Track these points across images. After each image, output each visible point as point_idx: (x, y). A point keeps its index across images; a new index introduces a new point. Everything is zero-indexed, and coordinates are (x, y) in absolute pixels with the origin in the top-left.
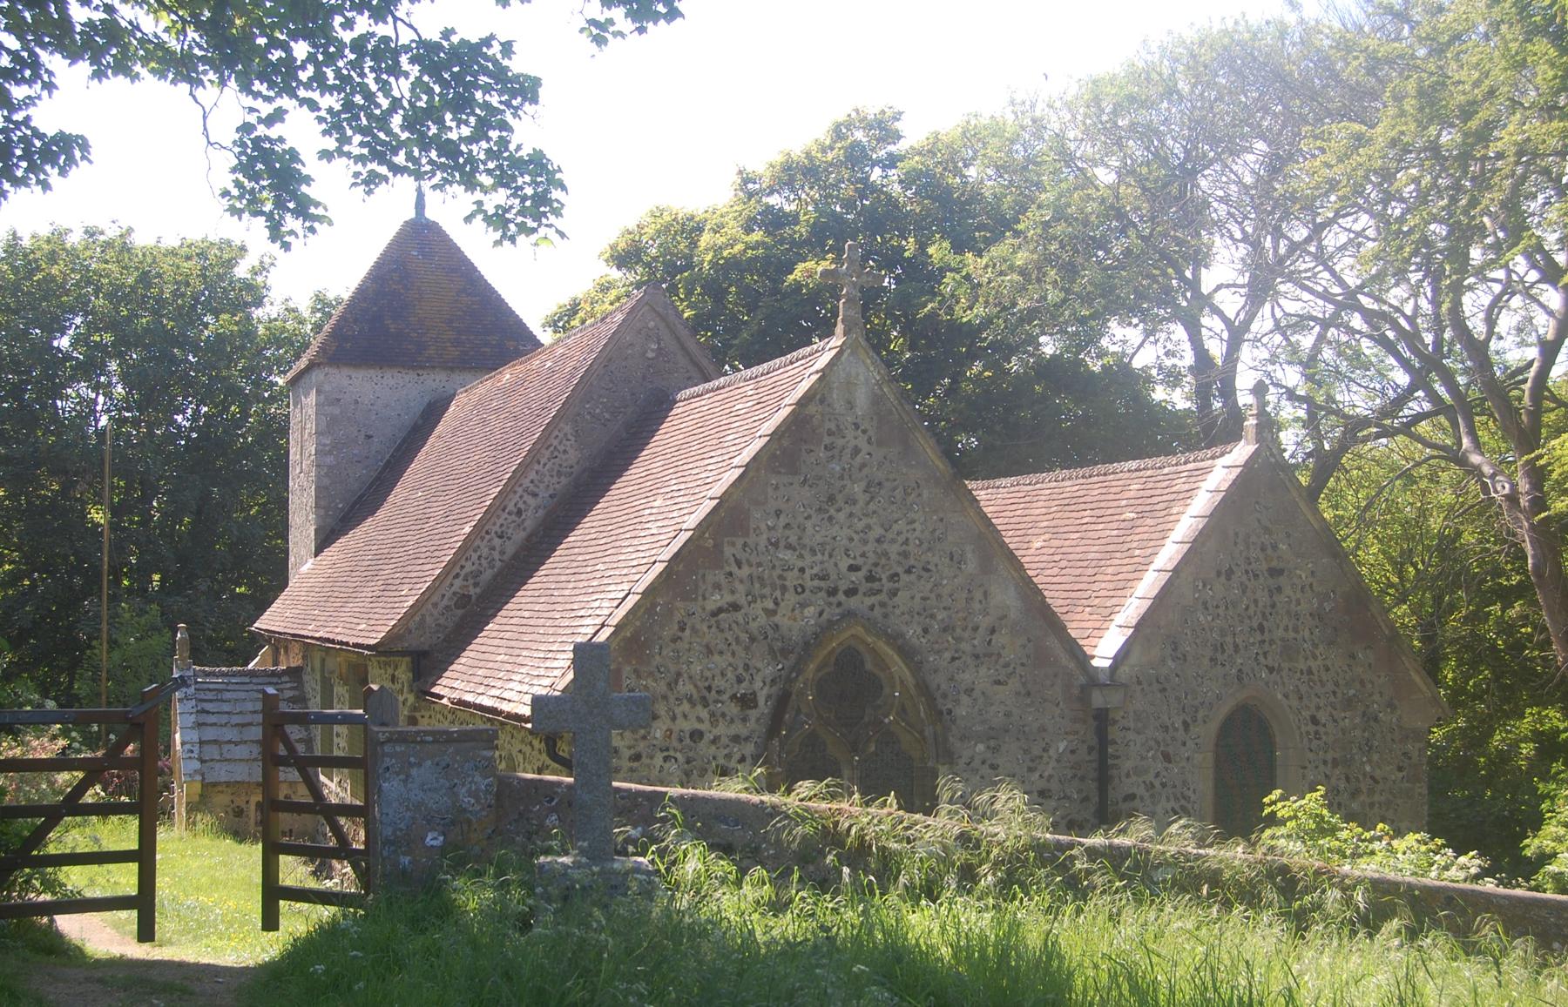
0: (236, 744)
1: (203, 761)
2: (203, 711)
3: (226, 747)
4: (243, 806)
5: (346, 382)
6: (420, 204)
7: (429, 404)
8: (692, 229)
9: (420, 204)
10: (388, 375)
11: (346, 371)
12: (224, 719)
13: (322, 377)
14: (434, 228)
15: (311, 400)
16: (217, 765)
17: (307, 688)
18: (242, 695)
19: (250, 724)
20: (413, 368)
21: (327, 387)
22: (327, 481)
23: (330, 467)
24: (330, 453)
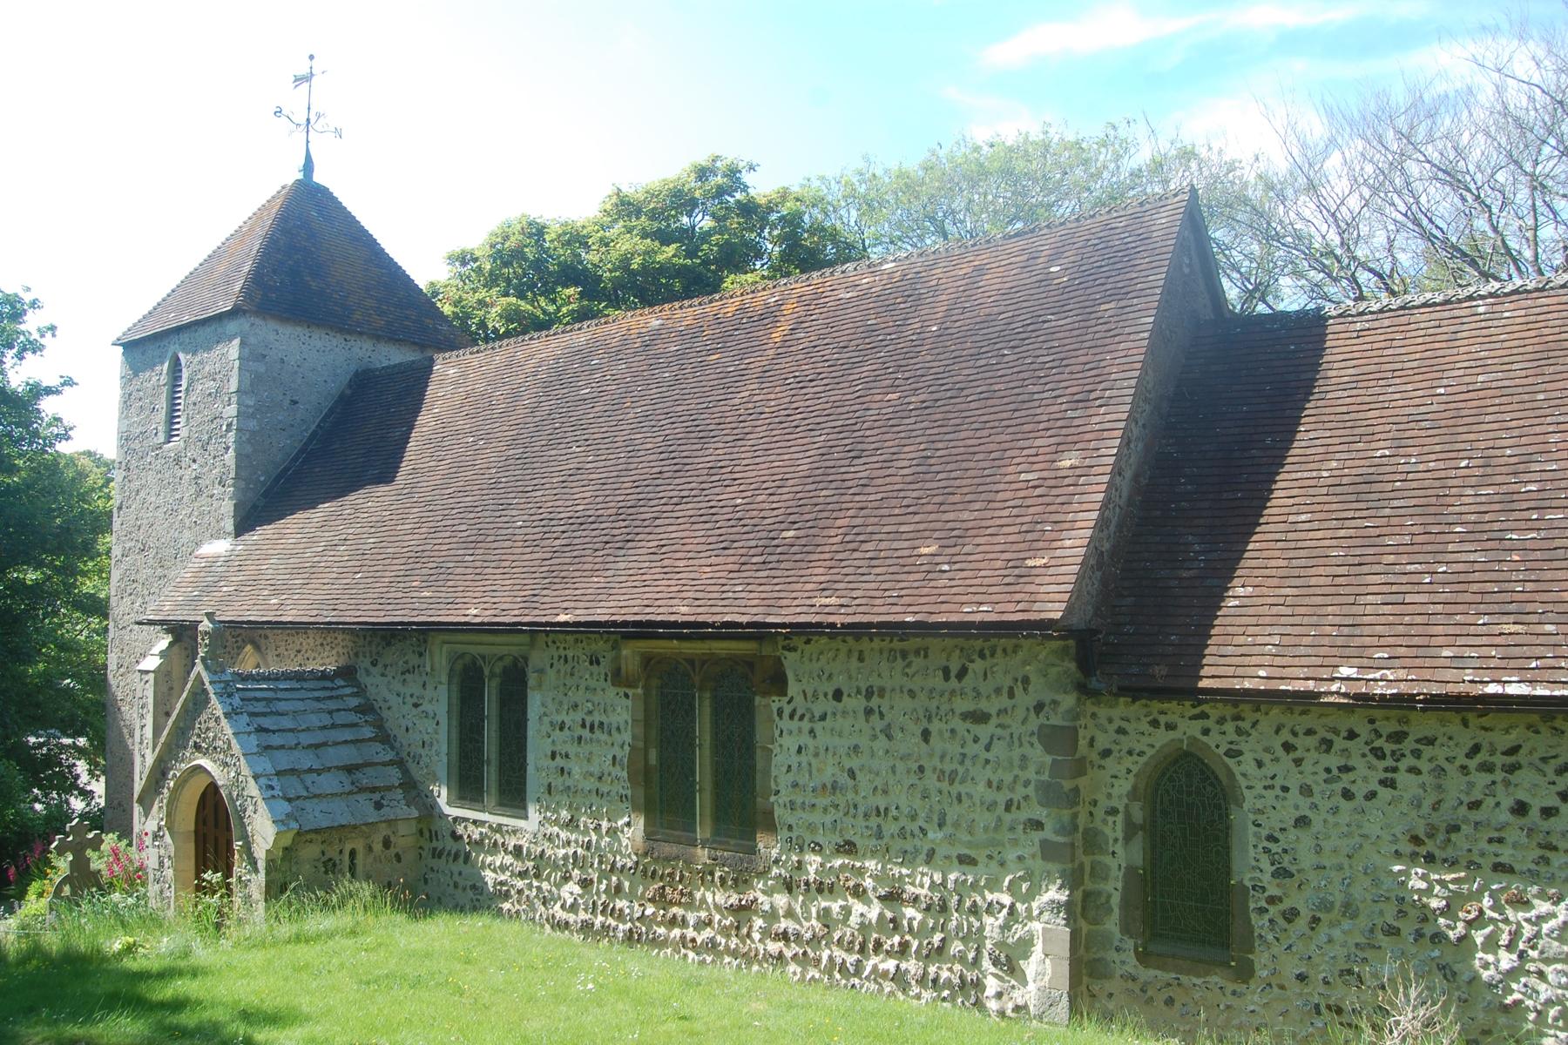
0: (319, 772)
1: (289, 800)
2: (261, 730)
3: (309, 778)
4: (337, 858)
5: (272, 337)
6: (308, 166)
7: (357, 374)
8: (576, 239)
9: (308, 166)
10: (316, 336)
11: (273, 325)
12: (290, 739)
13: (247, 326)
14: (324, 192)
15: (233, 350)
16: (308, 805)
17: (372, 691)
18: (300, 706)
19: (325, 744)
20: (341, 331)
21: (252, 340)
22: (249, 449)
23: (253, 433)
24: (253, 416)
